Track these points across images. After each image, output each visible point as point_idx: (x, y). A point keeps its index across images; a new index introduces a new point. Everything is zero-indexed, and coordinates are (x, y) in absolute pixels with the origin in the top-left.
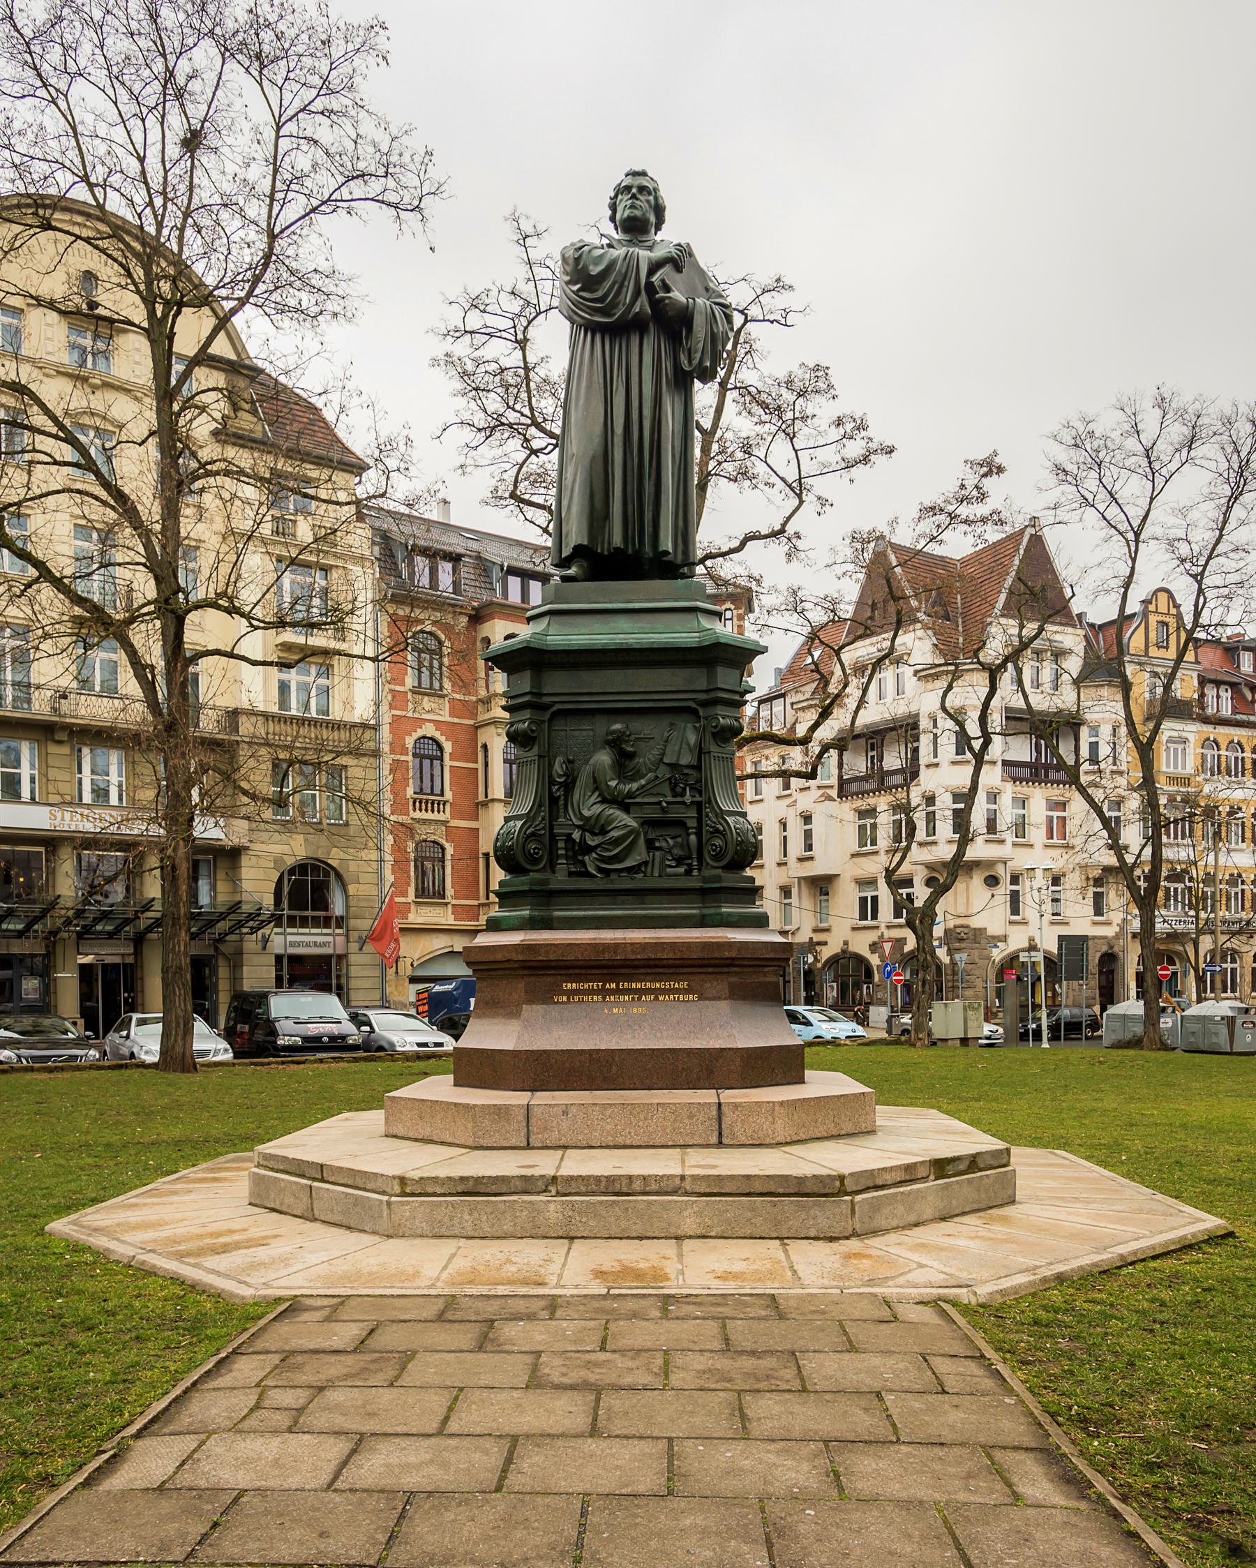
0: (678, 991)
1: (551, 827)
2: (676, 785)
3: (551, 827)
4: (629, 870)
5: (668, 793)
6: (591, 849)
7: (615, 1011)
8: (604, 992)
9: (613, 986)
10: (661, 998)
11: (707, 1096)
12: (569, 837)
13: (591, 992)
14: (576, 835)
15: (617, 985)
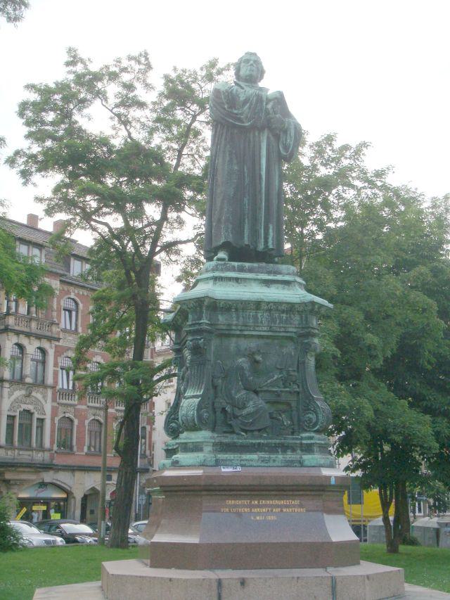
0: (294, 506)
1: (213, 403)
2: (286, 381)
3: (213, 403)
4: (259, 430)
5: (283, 386)
6: (236, 417)
7: (258, 518)
8: (251, 506)
9: (256, 502)
10: (284, 510)
11: (319, 572)
12: (224, 410)
13: (244, 506)
14: (228, 409)
15: (259, 502)
